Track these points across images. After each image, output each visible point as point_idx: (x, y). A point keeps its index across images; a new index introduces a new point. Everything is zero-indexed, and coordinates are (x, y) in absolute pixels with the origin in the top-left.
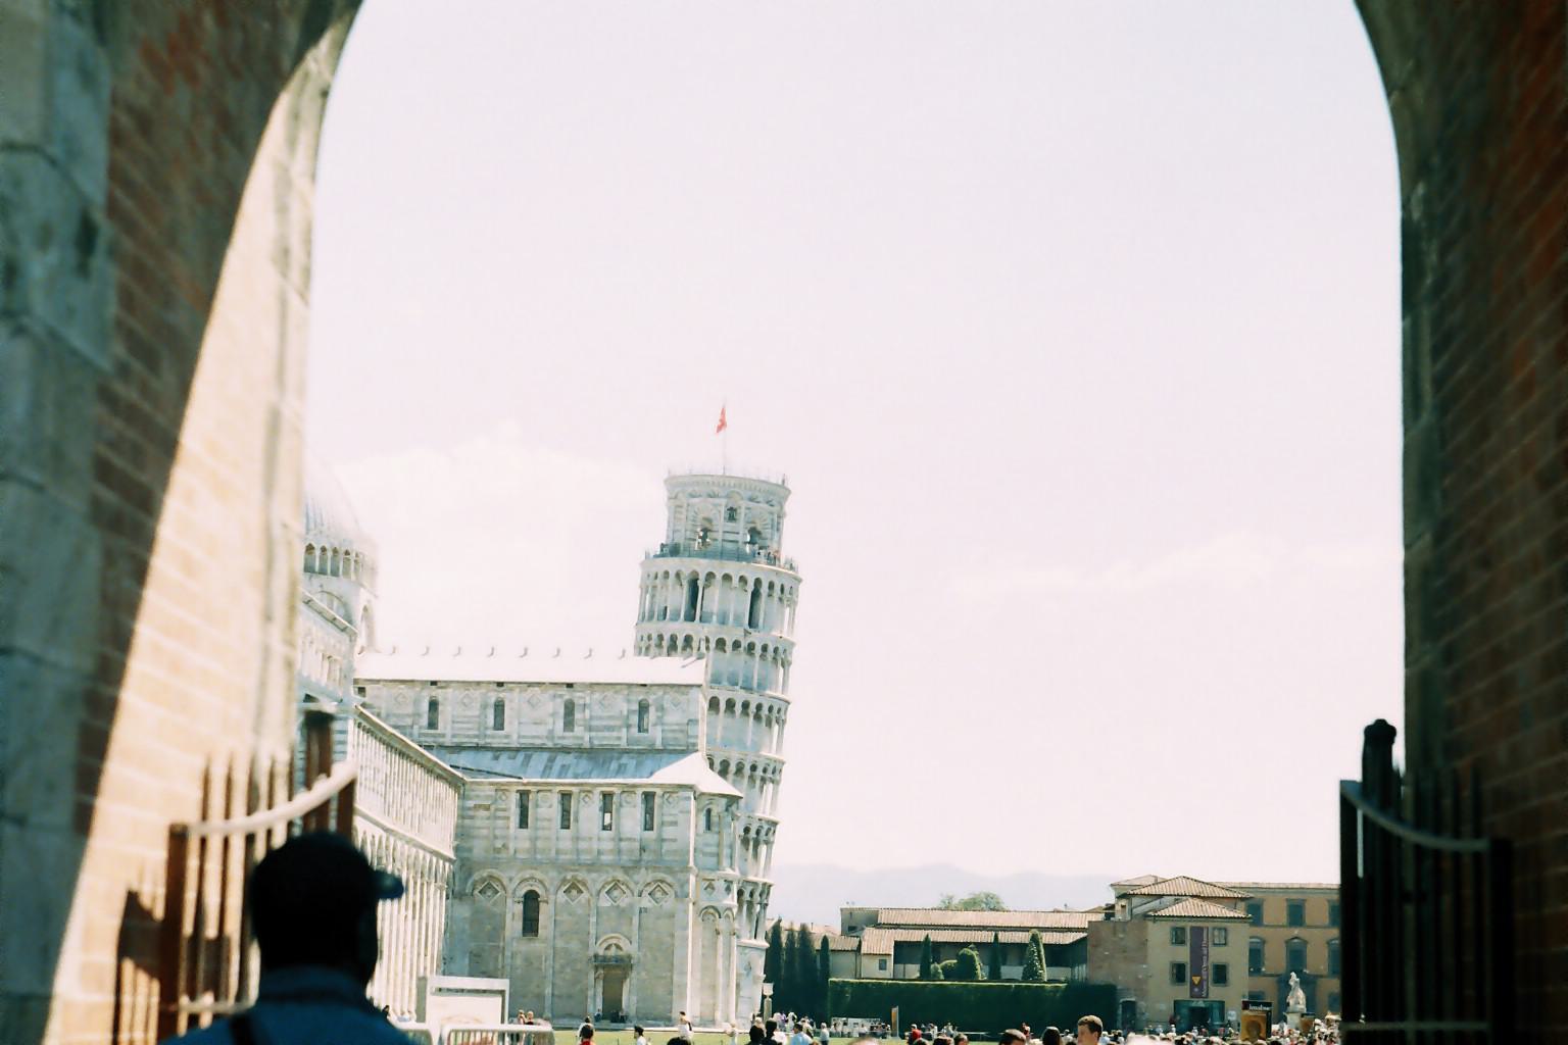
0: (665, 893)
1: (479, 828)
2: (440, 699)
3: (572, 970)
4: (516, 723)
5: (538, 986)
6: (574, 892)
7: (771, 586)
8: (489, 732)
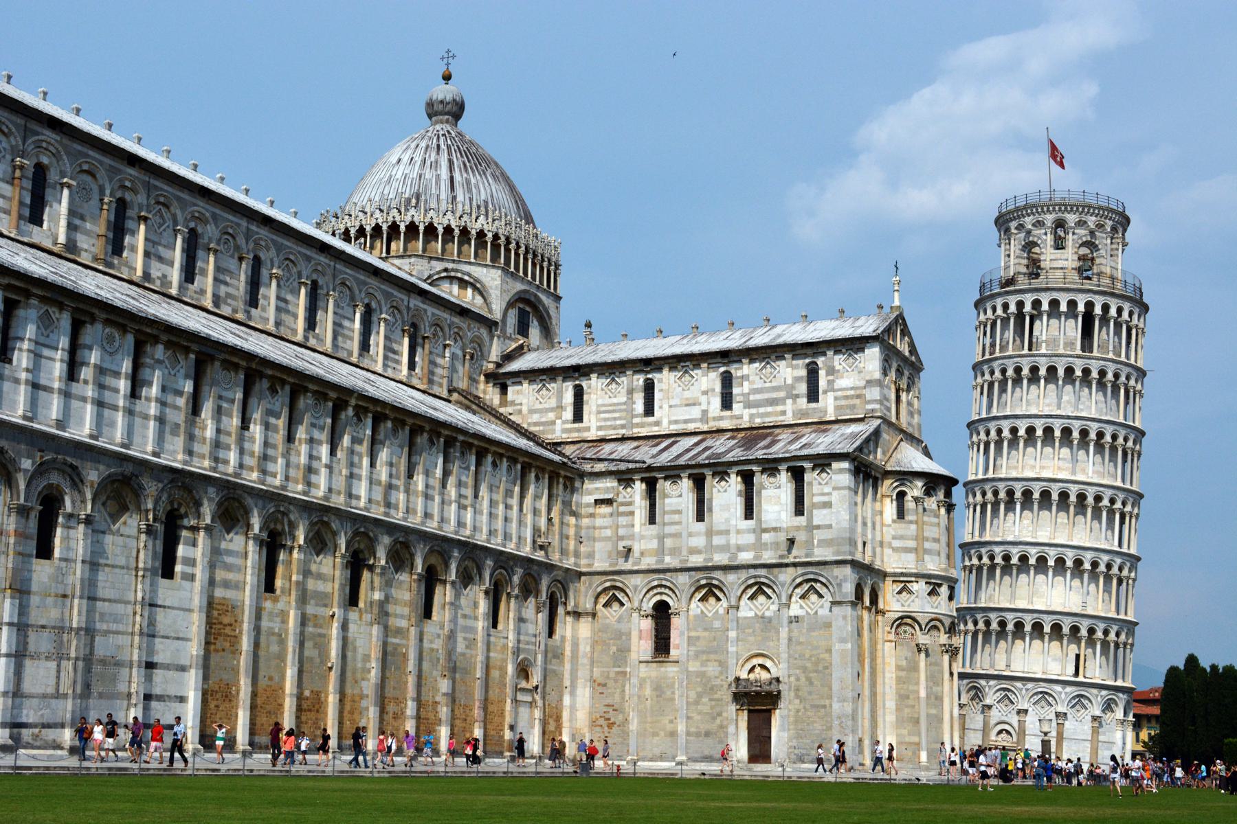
0: (821, 596)
1: (601, 528)
2: (585, 388)
3: (711, 700)
4: (666, 406)
5: (671, 722)
6: (712, 600)
7: (1106, 308)
8: (636, 420)
